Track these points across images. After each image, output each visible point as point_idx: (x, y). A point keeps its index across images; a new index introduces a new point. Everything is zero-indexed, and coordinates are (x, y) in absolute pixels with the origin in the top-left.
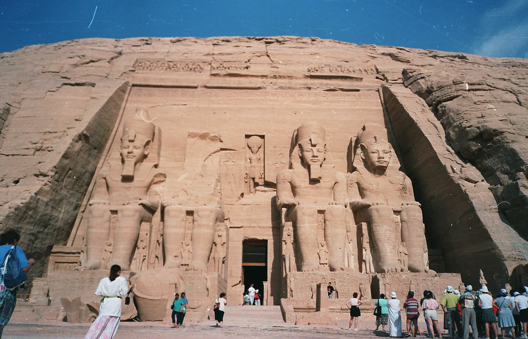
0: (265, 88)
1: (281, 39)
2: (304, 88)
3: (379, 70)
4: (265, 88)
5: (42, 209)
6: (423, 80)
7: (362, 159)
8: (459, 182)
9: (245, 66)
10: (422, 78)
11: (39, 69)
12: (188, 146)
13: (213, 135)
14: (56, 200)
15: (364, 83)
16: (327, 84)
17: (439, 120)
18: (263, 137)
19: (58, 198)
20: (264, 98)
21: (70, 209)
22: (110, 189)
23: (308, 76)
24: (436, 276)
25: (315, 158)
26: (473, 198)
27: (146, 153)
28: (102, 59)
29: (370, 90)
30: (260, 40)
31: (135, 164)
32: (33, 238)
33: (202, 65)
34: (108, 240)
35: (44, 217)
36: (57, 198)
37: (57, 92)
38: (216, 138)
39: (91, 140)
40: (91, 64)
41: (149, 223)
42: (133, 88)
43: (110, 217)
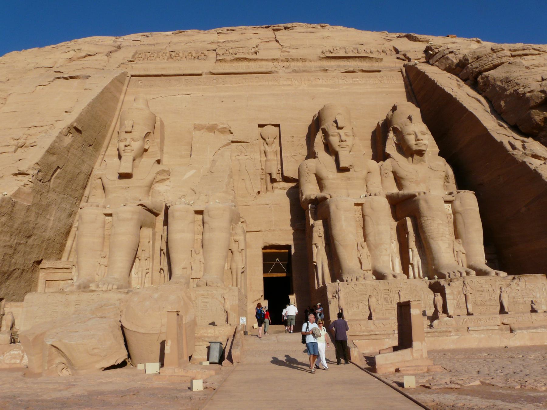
0: (277, 72)
1: (288, 25)
2: (320, 70)
3: (399, 50)
4: (277, 72)
5: (20, 216)
6: (453, 55)
7: (396, 144)
8: (525, 160)
9: (253, 50)
11: (33, 65)
12: (194, 139)
13: (221, 126)
16: (345, 66)
17: (480, 94)
18: (278, 126)
19: (44, 202)
20: (276, 83)
21: (63, 216)
23: (323, 58)
24: (514, 278)
27: (146, 147)
28: (100, 53)
29: (393, 70)
30: (266, 27)
31: (134, 160)
32: (10, 251)
33: (206, 53)
35: (25, 226)
37: (49, 86)
40: (89, 58)
41: (150, 230)
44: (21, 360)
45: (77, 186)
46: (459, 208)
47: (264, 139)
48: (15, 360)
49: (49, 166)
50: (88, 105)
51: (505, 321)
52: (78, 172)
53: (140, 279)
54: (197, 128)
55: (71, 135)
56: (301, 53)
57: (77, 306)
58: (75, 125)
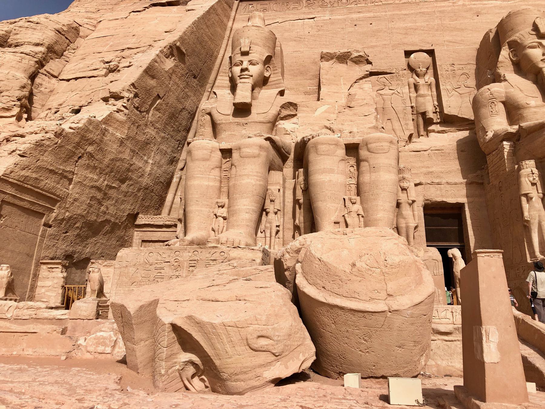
5: (113, 148)
13: (356, 54)
14: (138, 142)
18: (431, 53)
22: (219, 127)
27: (267, 74)
31: (253, 89)
32: (99, 196)
34: (219, 197)
35: (118, 164)
38: (362, 59)
42: (240, 3)
43: (221, 161)
44: (114, 347)
45: (180, 126)
48: (103, 348)
49: (148, 91)
50: (194, 23)
53: (268, 239)
54: (326, 57)
55: (173, 58)
57: (191, 269)
58: (178, 44)
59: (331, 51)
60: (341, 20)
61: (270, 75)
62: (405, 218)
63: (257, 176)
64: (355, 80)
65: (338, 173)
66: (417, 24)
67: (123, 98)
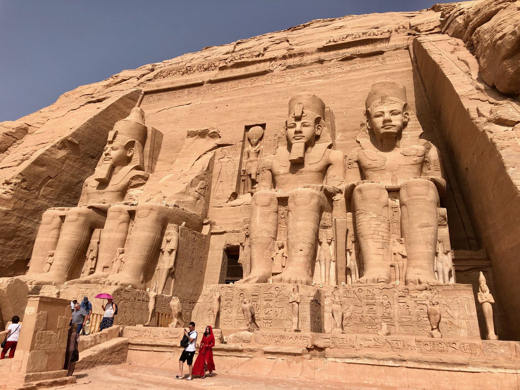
0: (272, 71)
4: (272, 71)
7: (369, 129)
8: (485, 128)
9: (258, 53)
10: (460, 14)
12: (184, 146)
13: (212, 131)
15: (392, 43)
18: (263, 126)
19: (30, 207)
20: (269, 83)
25: (298, 135)
26: (502, 148)
27: (129, 155)
28: (133, 77)
36: (29, 208)
38: (216, 135)
39: (82, 148)
46: (405, 199)
47: (249, 140)
51: (320, 343)
52: (77, 181)
56: (305, 48)
58: (69, 139)
59: (194, 130)
60: (207, 104)
61: (132, 156)
62: (163, 262)
63: (73, 235)
64: (205, 152)
65: (116, 232)
66: (259, 104)
67: (11, 183)
